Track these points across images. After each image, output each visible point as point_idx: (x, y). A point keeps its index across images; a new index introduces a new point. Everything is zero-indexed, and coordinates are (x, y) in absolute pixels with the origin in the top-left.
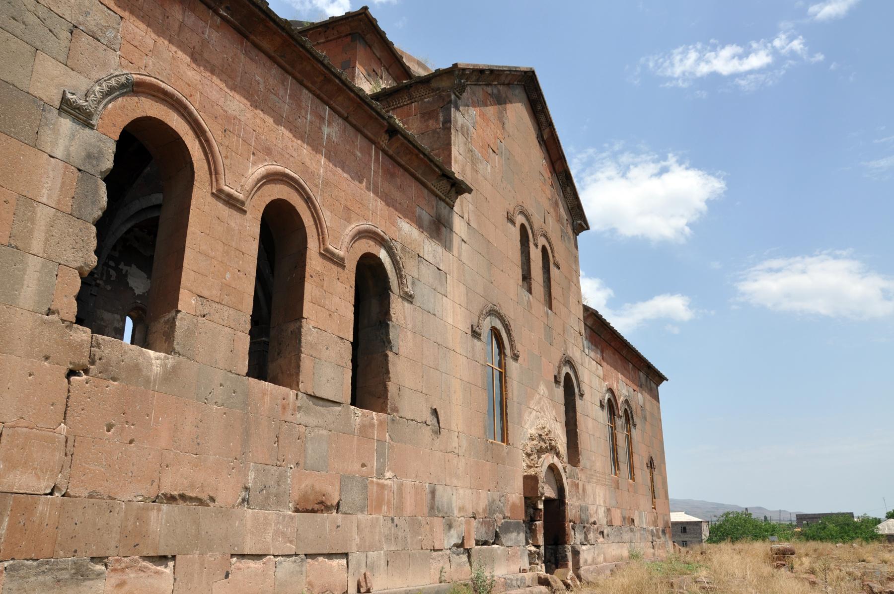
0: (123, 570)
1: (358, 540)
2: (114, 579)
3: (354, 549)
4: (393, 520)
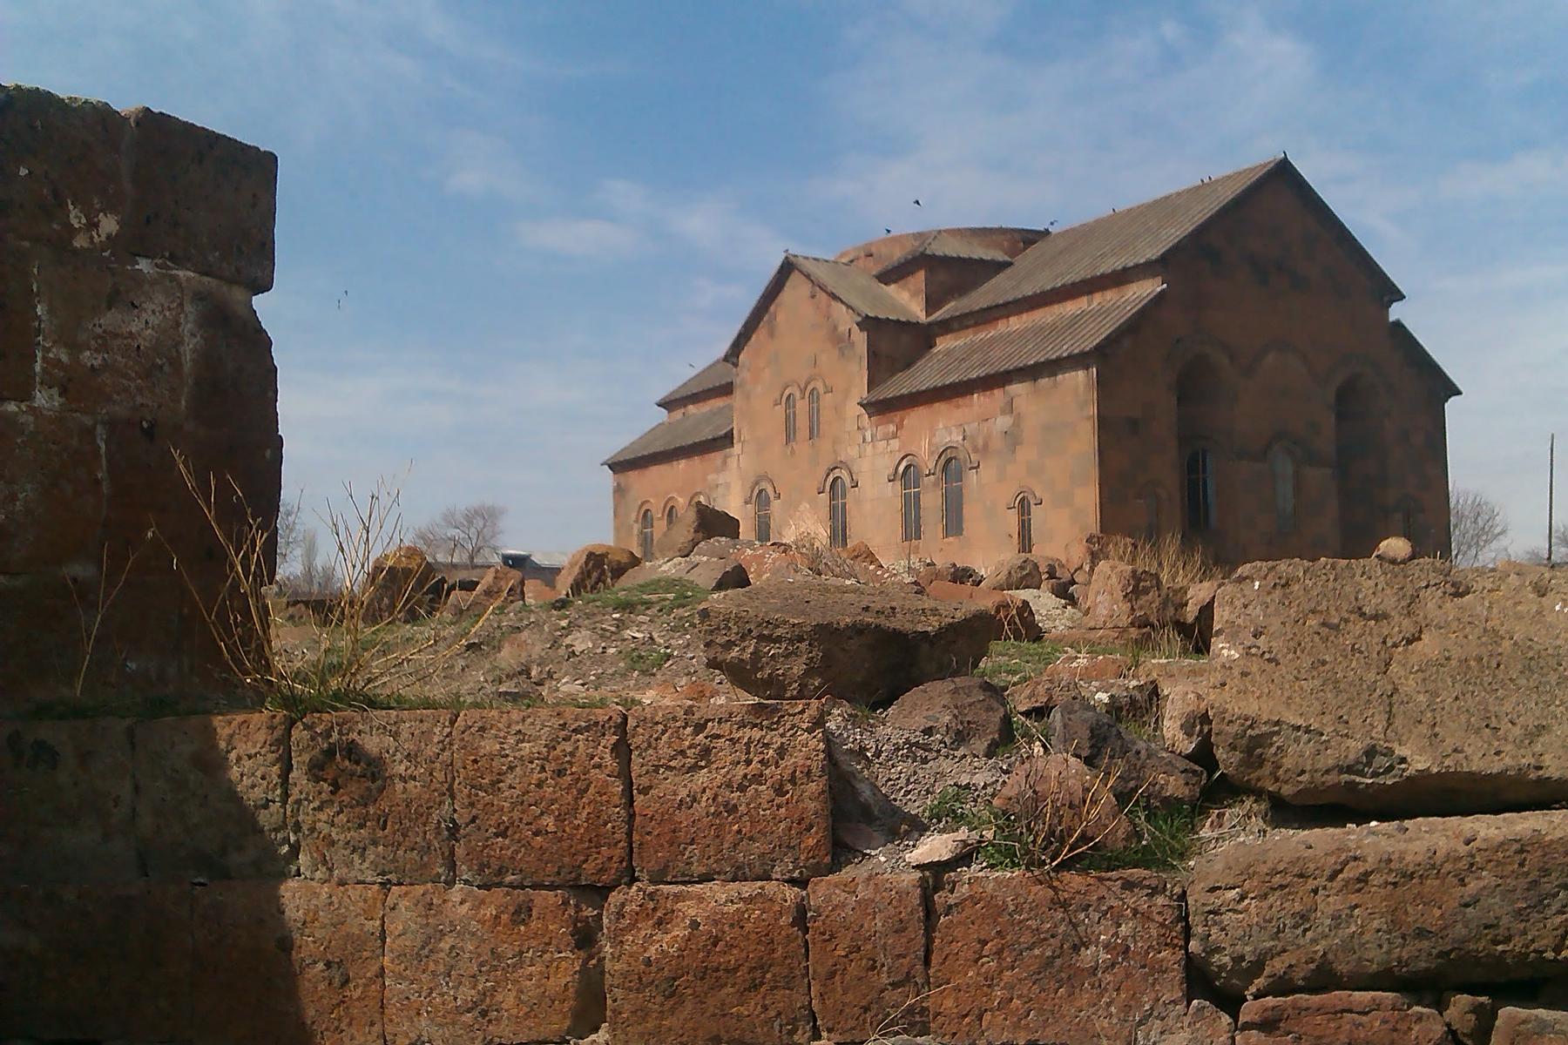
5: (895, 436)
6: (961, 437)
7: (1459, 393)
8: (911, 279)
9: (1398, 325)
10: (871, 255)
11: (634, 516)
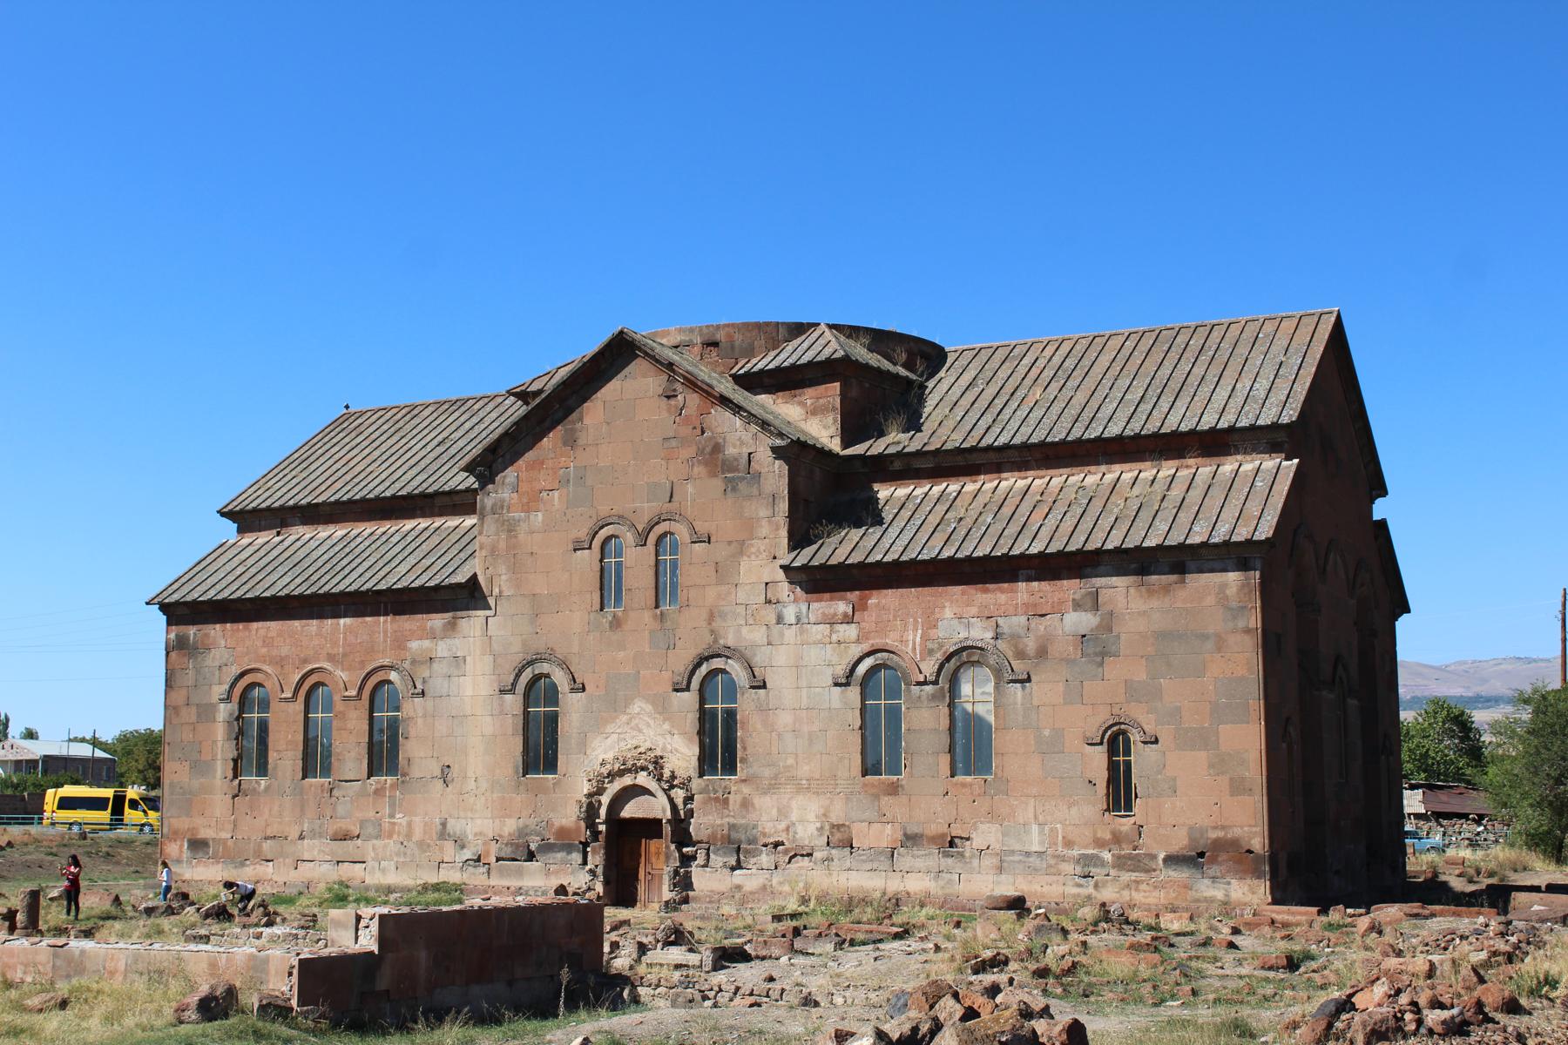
0: (255, 864)
1: (372, 854)
2: (252, 867)
3: (370, 859)
4: (402, 843)
5: (847, 619)
6: (989, 635)
9: (1382, 525)
10: (715, 344)
11: (220, 690)
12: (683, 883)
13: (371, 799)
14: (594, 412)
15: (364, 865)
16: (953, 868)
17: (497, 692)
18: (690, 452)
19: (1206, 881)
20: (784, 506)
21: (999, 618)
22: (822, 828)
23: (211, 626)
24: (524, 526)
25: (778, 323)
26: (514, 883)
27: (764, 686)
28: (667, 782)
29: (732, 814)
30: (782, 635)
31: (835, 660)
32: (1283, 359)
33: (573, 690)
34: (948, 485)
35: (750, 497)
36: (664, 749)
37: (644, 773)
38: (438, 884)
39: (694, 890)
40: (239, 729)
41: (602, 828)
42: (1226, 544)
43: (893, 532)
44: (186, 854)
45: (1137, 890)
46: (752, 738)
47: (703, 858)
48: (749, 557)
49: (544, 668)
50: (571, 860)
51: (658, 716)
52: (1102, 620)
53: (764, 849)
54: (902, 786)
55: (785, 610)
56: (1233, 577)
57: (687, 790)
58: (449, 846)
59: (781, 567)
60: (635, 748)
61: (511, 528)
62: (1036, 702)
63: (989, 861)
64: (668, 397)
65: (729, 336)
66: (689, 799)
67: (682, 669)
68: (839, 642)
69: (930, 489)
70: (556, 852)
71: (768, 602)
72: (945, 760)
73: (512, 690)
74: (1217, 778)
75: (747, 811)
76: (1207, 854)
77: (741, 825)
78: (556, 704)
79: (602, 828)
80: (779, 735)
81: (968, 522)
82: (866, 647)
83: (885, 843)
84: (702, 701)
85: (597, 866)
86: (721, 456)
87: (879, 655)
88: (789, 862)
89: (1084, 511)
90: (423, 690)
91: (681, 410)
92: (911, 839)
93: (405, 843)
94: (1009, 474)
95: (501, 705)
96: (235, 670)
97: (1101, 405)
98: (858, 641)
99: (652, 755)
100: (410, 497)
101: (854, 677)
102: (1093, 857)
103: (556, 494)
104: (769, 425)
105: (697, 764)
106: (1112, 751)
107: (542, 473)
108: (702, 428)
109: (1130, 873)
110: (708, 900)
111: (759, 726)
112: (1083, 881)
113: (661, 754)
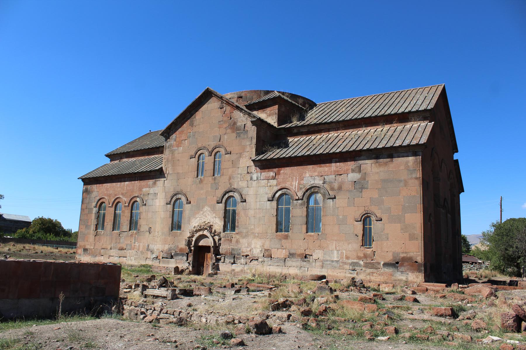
2: (98, 257)
4: (137, 252)
5: (274, 178)
6: (321, 182)
7: (464, 191)
8: (269, 109)
10: (241, 97)
12: (216, 268)
13: (129, 237)
14: (199, 115)
15: (126, 258)
16: (306, 266)
17: (166, 204)
18: (227, 125)
19: (399, 273)
20: (254, 141)
21: (325, 176)
22: (262, 250)
23: (94, 185)
24: (176, 152)
25: (261, 90)
26: (166, 266)
27: (245, 201)
28: (213, 233)
29: (233, 245)
30: (252, 184)
31: (269, 192)
32: (427, 95)
33: (187, 203)
34: (312, 137)
35: (244, 139)
36: (213, 223)
37: (206, 231)
38: (144, 265)
39: (220, 270)
40: (98, 216)
41: (193, 248)
42: (409, 146)
43: (291, 149)
44: (82, 253)
45: (372, 276)
46: (241, 219)
47: (223, 260)
48: (243, 158)
49: (179, 196)
50: (183, 259)
51: (212, 211)
52: (362, 176)
53: (243, 257)
54: (289, 236)
55: (253, 176)
56: (411, 159)
57: (219, 237)
58: (149, 253)
59: (252, 160)
60: (204, 222)
61: (173, 152)
62: (337, 206)
63: (318, 264)
64: (221, 108)
65: (245, 94)
66: (220, 239)
67: (220, 196)
68: (270, 186)
69: (306, 138)
70: (179, 256)
71: (248, 173)
72: (304, 227)
73: (170, 204)
74: (404, 234)
75: (238, 244)
76: (399, 263)
77: (236, 249)
78: (182, 208)
79: (193, 248)
80: (249, 218)
81: (317, 145)
82: (279, 187)
83: (282, 256)
84: (226, 207)
85: (190, 261)
86: (236, 125)
87: (283, 190)
88: (250, 262)
89: (357, 140)
90: (145, 204)
91: (225, 112)
92: (292, 255)
93: (138, 252)
94: (332, 132)
95: (166, 208)
96: (98, 198)
97: (364, 110)
98: (277, 185)
99: (209, 225)
100: (152, 148)
101: (275, 198)
102: (356, 263)
103: (186, 141)
104: (251, 114)
105: (223, 228)
106: (364, 224)
107: (183, 134)
108: (231, 117)
109: (370, 269)
110: (223, 274)
111: (243, 215)
112: (352, 272)
113: (212, 224)
